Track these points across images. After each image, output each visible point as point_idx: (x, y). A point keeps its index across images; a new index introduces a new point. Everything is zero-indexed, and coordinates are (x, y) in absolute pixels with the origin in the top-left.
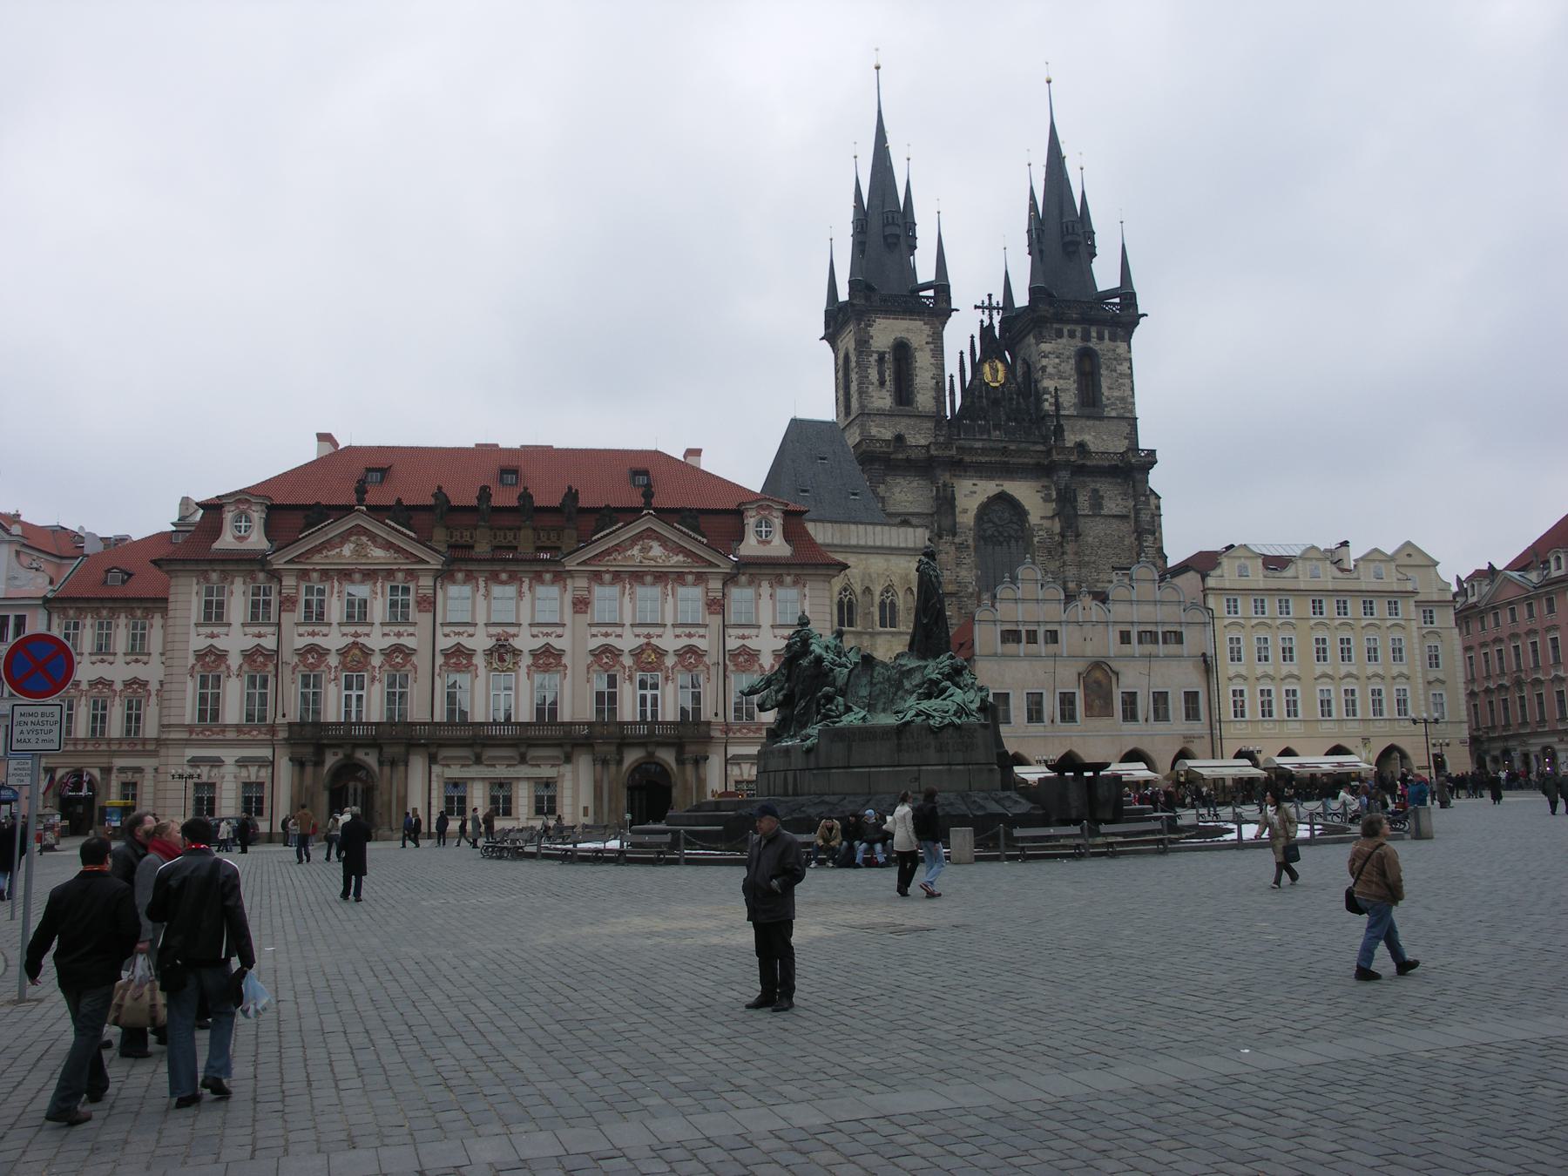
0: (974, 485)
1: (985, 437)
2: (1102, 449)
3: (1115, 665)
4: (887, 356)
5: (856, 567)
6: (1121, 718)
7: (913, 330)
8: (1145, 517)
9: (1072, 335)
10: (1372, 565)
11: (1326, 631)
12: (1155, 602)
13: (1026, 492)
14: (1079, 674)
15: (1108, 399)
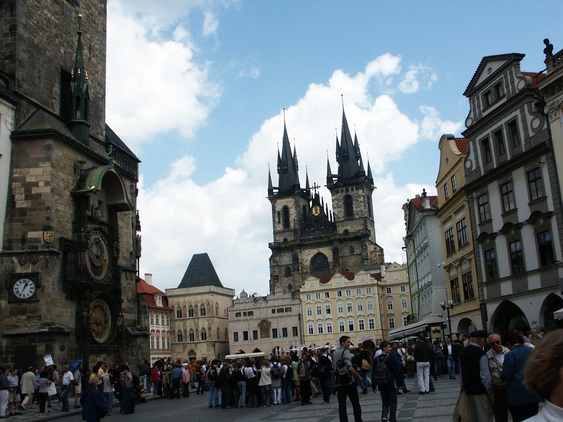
0: (310, 251)
1: (313, 234)
2: (353, 231)
3: (270, 320)
4: (281, 212)
5: (192, 300)
6: (292, 334)
7: (289, 202)
8: (364, 254)
9: (342, 191)
10: (360, 276)
11: (342, 302)
12: (282, 299)
13: (327, 251)
14: (258, 324)
15: (356, 212)
